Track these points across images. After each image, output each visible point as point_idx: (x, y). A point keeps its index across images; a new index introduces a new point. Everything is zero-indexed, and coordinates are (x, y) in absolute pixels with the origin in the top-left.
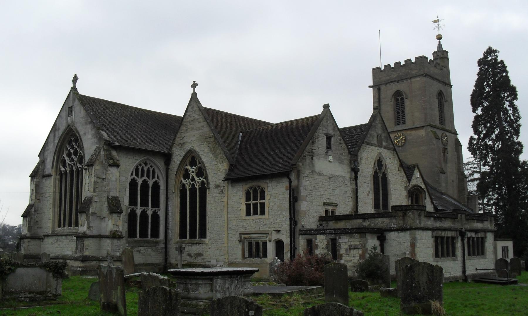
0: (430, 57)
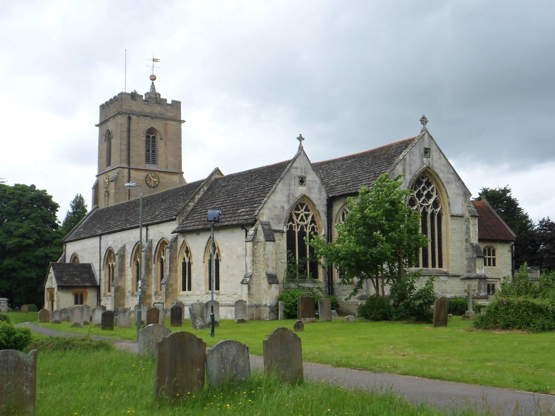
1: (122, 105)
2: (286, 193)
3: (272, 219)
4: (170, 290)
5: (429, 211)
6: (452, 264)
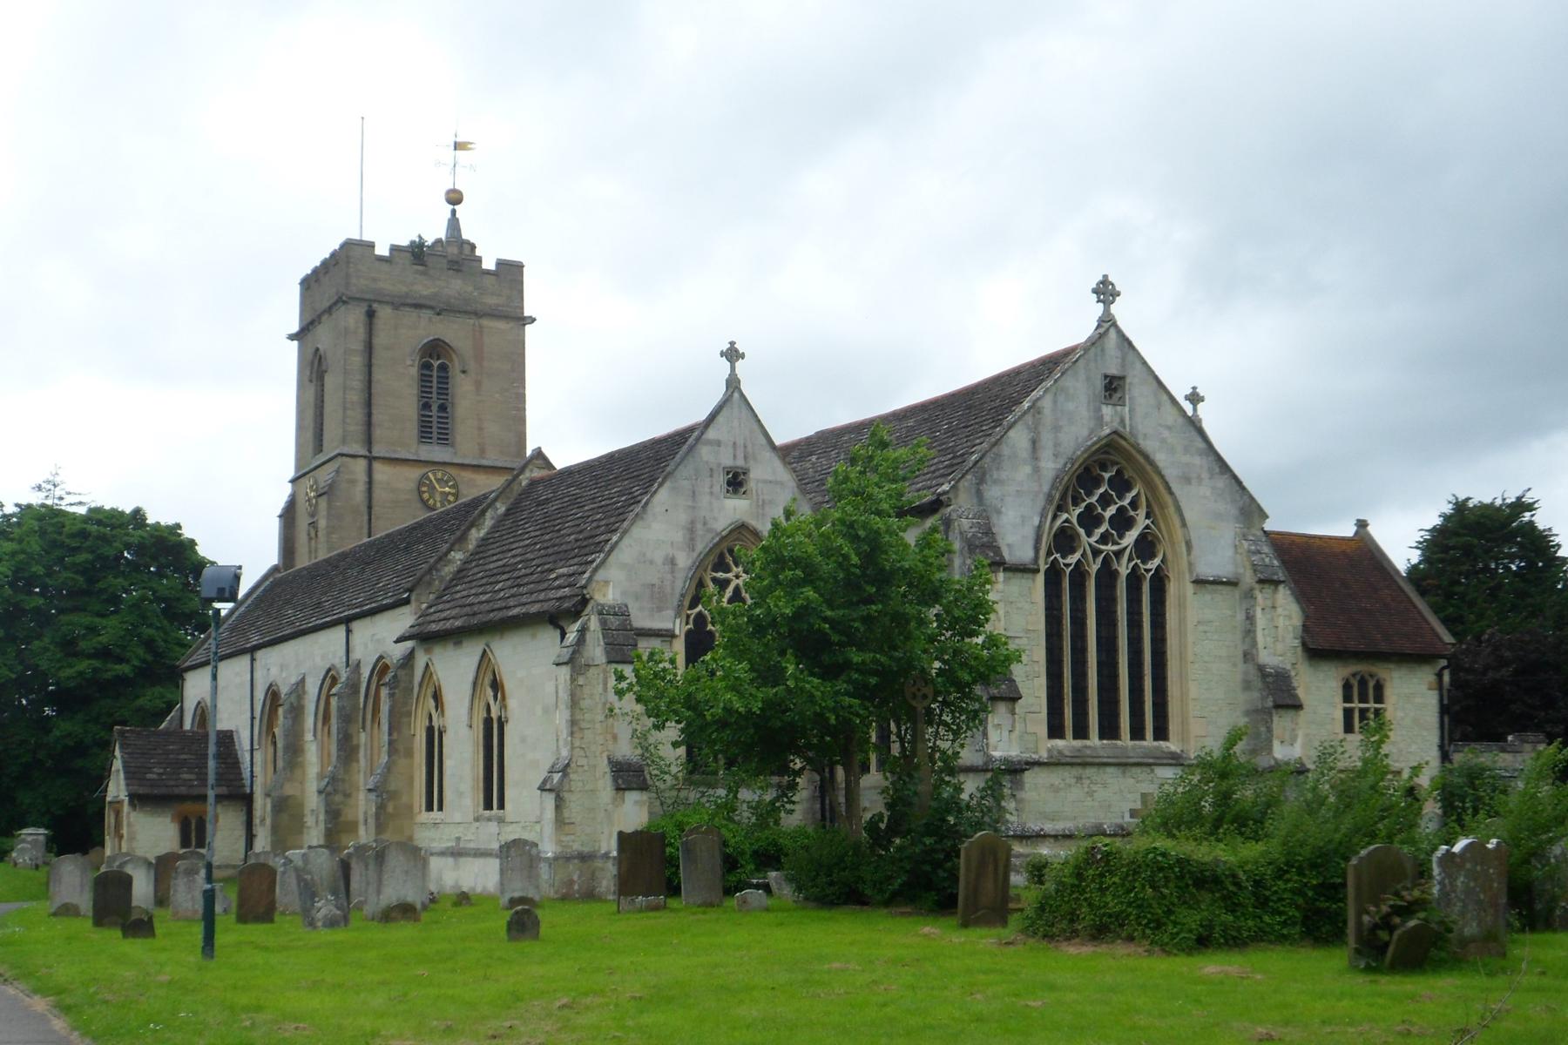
0: (489, 264)
1: (348, 276)
2: (683, 517)
3: (637, 597)
4: (390, 809)
5: (1124, 570)
6: (1196, 728)
